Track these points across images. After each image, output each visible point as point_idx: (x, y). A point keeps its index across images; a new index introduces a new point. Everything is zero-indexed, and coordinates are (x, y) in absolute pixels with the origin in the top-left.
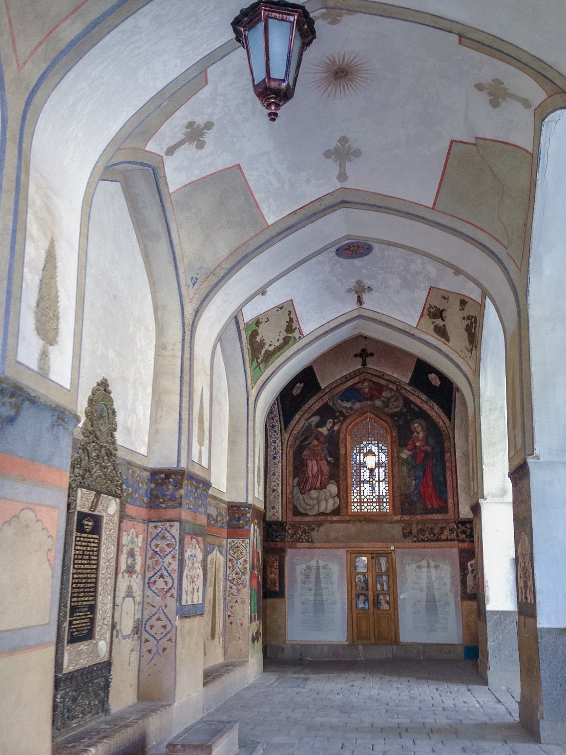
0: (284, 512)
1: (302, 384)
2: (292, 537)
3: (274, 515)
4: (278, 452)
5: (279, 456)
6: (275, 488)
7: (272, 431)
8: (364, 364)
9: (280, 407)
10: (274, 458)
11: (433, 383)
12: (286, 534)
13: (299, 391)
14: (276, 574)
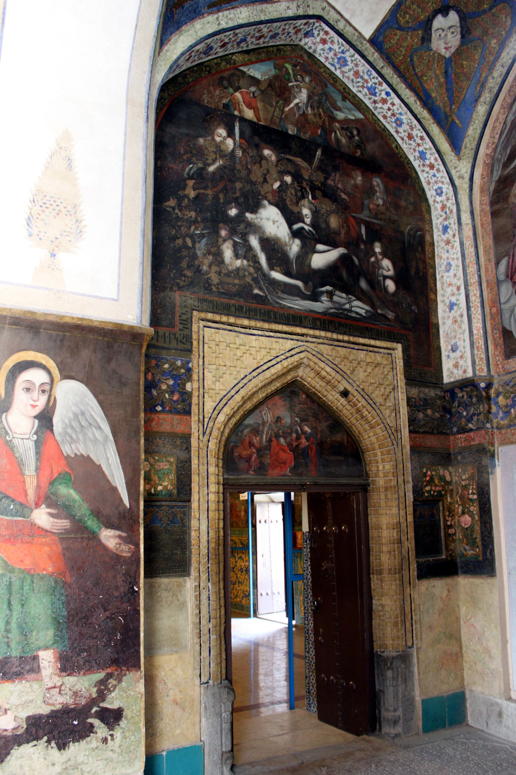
0: (481, 354)
2: (507, 413)
3: (456, 366)
4: (451, 211)
5: (453, 220)
6: (453, 299)
7: (427, 169)
10: (445, 229)
12: (494, 409)
13: (454, 40)
14: (472, 516)
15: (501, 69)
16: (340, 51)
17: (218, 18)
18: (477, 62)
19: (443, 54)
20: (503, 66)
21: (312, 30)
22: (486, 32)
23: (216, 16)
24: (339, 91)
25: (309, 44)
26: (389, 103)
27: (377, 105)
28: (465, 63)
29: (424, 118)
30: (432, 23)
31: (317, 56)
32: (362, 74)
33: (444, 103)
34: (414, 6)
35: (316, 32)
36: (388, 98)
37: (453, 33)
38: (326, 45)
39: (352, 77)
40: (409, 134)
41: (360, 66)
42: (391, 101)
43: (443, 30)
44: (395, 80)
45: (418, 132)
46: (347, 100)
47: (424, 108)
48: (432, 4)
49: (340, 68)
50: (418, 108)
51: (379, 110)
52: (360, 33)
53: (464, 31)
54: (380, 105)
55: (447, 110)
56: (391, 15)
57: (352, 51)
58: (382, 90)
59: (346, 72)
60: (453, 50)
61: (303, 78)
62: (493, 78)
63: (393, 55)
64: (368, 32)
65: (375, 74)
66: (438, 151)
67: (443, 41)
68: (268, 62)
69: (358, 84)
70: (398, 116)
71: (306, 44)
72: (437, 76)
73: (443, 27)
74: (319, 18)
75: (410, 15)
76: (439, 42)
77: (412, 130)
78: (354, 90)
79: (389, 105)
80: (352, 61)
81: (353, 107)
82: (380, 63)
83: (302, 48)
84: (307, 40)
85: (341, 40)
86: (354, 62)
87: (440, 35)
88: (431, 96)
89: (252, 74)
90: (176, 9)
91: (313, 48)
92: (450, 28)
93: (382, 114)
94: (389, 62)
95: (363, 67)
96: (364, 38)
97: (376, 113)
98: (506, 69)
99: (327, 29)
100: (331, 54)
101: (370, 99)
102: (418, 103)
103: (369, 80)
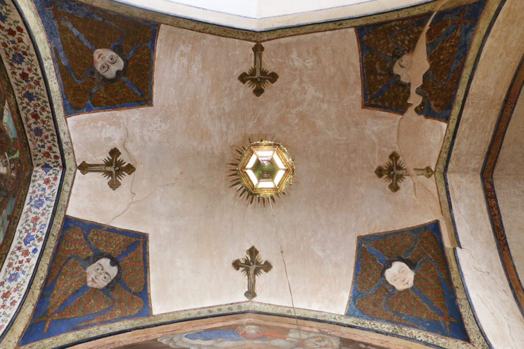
1: (114, 271)
8: (251, 293)
9: (42, 273)
11: (400, 287)
13: (101, 283)
15: (108, 329)
16: (47, 196)
17: (49, 58)
18: (99, 310)
19: (88, 280)
20: (110, 329)
21: (51, 168)
22: (120, 301)
23: (50, 57)
24: (14, 212)
25: (38, 174)
26: (27, 257)
27: (17, 252)
28: (92, 301)
29: (33, 293)
30: (101, 258)
31: (31, 185)
32: (38, 222)
33: (54, 305)
34: (104, 238)
35: (51, 172)
36: (31, 254)
37: (105, 277)
38: (45, 185)
39: (30, 218)
40: (8, 292)
41: (44, 217)
42: (30, 257)
43: (103, 270)
44: (49, 251)
45: (17, 297)
46: (9, 221)
47: (41, 289)
48: (113, 250)
49: (32, 206)
50: (39, 283)
51: (14, 257)
52: (67, 206)
53: (111, 285)
54: (18, 253)
55: (51, 311)
56: (90, 224)
57: (53, 204)
58: (35, 245)
59: (31, 212)
60: (95, 286)
61: (13, 169)
62: (98, 329)
63: (66, 241)
64: (71, 212)
65: (45, 231)
66: (12, 323)
67: (97, 274)
68: (16, 133)
69: (26, 226)
70: (20, 272)
71: (37, 172)
72: (71, 285)
73: (104, 268)
74: (64, 167)
75: (98, 238)
76: (94, 272)
77: (15, 291)
78: (19, 227)
79: (25, 259)
80: (45, 209)
81: (5, 230)
82: (55, 231)
83: (32, 170)
84: (41, 170)
85: (56, 191)
86: (45, 211)
87: (98, 269)
88: (53, 290)
89: (4, 112)
90: (53, 10)
91: (36, 178)
92: (107, 273)
93: (11, 261)
94: (59, 240)
95: (45, 220)
96: (65, 211)
97: (9, 256)
98: (111, 331)
99: (59, 177)
100: (40, 193)
101: (19, 243)
102: (42, 282)
103: (36, 231)
